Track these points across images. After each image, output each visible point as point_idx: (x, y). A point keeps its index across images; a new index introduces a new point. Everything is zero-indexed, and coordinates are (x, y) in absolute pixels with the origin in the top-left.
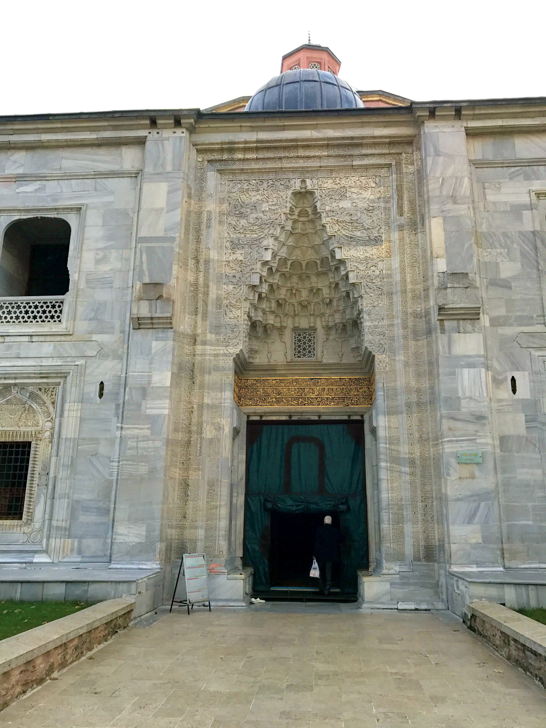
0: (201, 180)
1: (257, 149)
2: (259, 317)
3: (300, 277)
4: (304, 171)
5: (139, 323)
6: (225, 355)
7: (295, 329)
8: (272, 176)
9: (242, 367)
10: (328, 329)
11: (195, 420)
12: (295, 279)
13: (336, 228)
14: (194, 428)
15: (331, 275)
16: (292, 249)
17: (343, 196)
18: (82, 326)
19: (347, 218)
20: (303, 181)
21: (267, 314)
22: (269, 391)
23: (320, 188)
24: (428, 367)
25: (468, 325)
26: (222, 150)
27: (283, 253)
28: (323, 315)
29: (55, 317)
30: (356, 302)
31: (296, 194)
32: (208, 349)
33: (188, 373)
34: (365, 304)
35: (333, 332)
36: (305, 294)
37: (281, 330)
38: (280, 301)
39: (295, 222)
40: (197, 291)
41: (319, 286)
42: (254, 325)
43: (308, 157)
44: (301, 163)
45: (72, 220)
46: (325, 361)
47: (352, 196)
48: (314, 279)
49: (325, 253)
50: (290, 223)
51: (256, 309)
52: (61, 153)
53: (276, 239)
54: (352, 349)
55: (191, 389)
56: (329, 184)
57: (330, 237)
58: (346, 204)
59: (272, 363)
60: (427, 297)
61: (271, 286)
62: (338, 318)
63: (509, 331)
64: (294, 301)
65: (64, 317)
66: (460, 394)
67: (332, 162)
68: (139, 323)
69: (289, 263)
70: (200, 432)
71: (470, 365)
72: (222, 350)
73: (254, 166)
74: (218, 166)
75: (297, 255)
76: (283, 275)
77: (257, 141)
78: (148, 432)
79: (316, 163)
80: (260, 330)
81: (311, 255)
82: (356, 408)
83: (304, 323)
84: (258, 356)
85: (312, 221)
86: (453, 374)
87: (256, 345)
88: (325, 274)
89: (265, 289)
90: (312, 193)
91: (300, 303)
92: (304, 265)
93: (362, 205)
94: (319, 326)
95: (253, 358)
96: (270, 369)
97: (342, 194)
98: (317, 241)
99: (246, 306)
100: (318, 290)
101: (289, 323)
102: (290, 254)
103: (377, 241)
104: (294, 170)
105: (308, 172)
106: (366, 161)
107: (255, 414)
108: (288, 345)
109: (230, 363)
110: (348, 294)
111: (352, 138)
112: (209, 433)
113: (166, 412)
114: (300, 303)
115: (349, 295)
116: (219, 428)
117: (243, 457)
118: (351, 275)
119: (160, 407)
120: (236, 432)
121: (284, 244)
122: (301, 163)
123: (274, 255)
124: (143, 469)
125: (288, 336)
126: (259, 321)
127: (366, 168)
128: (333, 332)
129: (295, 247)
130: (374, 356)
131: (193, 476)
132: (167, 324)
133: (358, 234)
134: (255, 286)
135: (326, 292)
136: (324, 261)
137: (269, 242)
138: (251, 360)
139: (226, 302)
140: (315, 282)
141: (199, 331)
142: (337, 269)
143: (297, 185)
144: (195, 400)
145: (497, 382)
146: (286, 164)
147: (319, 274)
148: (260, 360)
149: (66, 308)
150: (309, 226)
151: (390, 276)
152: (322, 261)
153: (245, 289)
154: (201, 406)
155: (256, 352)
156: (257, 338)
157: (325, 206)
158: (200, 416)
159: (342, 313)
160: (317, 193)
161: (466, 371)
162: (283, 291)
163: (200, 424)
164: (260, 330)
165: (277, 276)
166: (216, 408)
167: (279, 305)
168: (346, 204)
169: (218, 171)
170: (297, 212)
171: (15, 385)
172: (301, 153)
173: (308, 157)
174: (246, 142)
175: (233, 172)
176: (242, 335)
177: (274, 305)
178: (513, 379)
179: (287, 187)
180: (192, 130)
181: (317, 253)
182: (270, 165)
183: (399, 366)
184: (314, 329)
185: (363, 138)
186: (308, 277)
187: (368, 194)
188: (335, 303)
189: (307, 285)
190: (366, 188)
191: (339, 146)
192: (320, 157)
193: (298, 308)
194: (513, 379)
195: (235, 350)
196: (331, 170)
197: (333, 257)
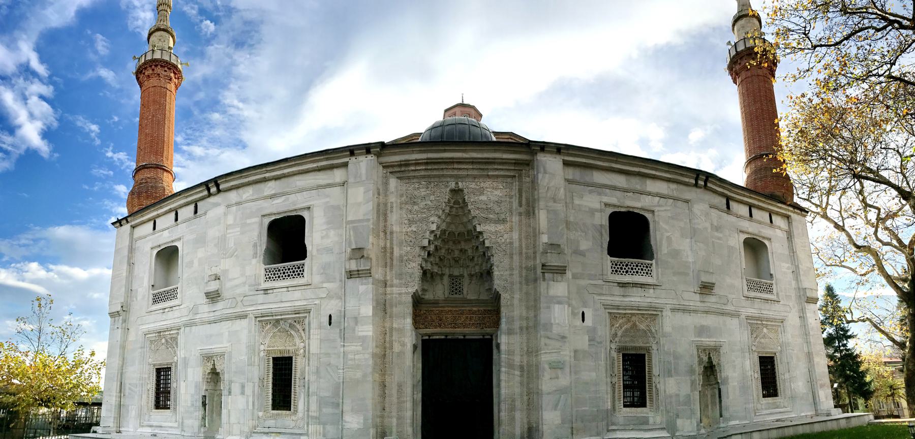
2: (429, 267)
3: (454, 242)
4: (457, 177)
5: (351, 275)
8: (437, 179)
9: (417, 301)
10: (471, 276)
11: (387, 339)
12: (451, 243)
13: (477, 212)
14: (388, 345)
15: (473, 241)
16: (449, 224)
17: (482, 193)
18: (316, 279)
19: (484, 207)
20: (457, 183)
22: (434, 317)
23: (467, 187)
24: (534, 304)
25: (559, 277)
27: (444, 226)
29: (300, 274)
30: (489, 259)
31: (452, 191)
32: (395, 290)
33: (383, 307)
34: (495, 260)
35: (474, 278)
36: (457, 253)
37: (442, 275)
39: (451, 207)
41: (466, 248)
42: (425, 272)
43: (460, 169)
44: (456, 172)
46: (468, 298)
47: (488, 195)
48: (463, 243)
49: (470, 227)
50: (448, 208)
51: (426, 261)
53: (439, 217)
55: (384, 318)
56: (473, 186)
57: (474, 217)
58: (483, 198)
60: (535, 258)
61: (436, 246)
62: (477, 269)
63: (583, 282)
65: (305, 274)
66: (552, 321)
67: (475, 173)
68: (351, 275)
70: (391, 348)
71: (559, 303)
72: (404, 290)
75: (453, 228)
76: (443, 240)
77: (427, 159)
78: (360, 348)
79: (465, 173)
80: (429, 275)
81: (461, 229)
82: (489, 330)
83: (456, 272)
85: (462, 208)
86: (549, 307)
88: (470, 240)
89: (432, 248)
90: (462, 190)
91: (454, 259)
93: (493, 198)
96: (435, 303)
97: (481, 192)
98: (465, 220)
99: (419, 260)
101: (447, 271)
102: (448, 227)
103: (504, 221)
104: (451, 176)
106: (496, 173)
107: (426, 335)
108: (446, 287)
109: (410, 299)
110: (484, 253)
112: (397, 348)
113: (371, 334)
114: (454, 259)
115: (486, 255)
116: (403, 345)
117: (420, 365)
118: (486, 242)
119: (367, 330)
120: (415, 347)
122: (456, 172)
123: (438, 228)
124: (359, 375)
125: (446, 279)
127: (497, 176)
128: (474, 278)
129: (450, 223)
131: (388, 379)
132: (368, 273)
133: (491, 216)
134: (424, 247)
135: (470, 251)
136: (469, 232)
139: (405, 258)
140: (463, 245)
141: (388, 278)
142: (478, 237)
143: (452, 185)
144: (387, 325)
145: (574, 314)
146: (445, 172)
147: (466, 241)
148: (429, 296)
149: (306, 268)
150: (460, 210)
152: (468, 232)
154: (391, 329)
156: (427, 281)
157: (470, 199)
158: (391, 336)
160: (465, 191)
161: (557, 306)
162: (443, 251)
163: (391, 342)
164: (429, 275)
165: (440, 241)
166: (401, 331)
167: (441, 260)
168: (483, 198)
170: (452, 201)
172: (456, 166)
173: (460, 169)
176: (417, 279)
177: (437, 259)
179: (447, 186)
182: (435, 173)
183: (516, 302)
184: (462, 276)
185: (495, 159)
186: (459, 242)
187: (498, 193)
188: (476, 259)
190: (496, 189)
191: (479, 163)
192: (467, 169)
193: (452, 262)
194: (583, 314)
195: (412, 290)
196: (475, 177)
197: (475, 230)
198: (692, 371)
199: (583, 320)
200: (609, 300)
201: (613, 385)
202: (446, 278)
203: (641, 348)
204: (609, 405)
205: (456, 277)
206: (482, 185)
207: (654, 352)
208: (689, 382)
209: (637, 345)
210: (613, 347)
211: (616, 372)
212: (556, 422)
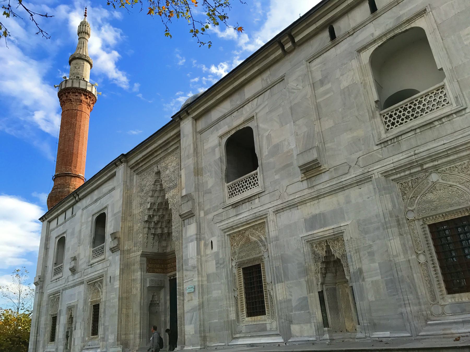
0: (131, 180)
1: (144, 159)
2: (159, 231)
6: (138, 255)
26: (136, 165)
40: (131, 229)
45: (105, 211)
52: (103, 186)
53: (152, 196)
69: (164, 203)
73: (144, 167)
74: (137, 172)
77: (142, 157)
87: (164, 244)
93: (172, 170)
105: (158, 162)
111: (165, 141)
112: (134, 291)
116: (137, 289)
121: (158, 197)
137: (149, 199)
138: (165, 251)
143: (156, 170)
146: (152, 162)
151: (179, 201)
153: (143, 223)
168: (168, 172)
169: (137, 174)
171: (96, 282)
174: (140, 159)
175: (140, 173)
178: (212, 242)
180: (127, 162)
182: (148, 164)
185: (168, 139)
192: (159, 154)
196: (164, 157)
198: (306, 271)
199: (212, 248)
200: (224, 224)
201: (236, 299)
203: (254, 259)
204: (233, 316)
206: (167, 162)
207: (266, 260)
208: (304, 283)
209: (251, 257)
210: (234, 265)
211: (238, 286)
212: (191, 333)
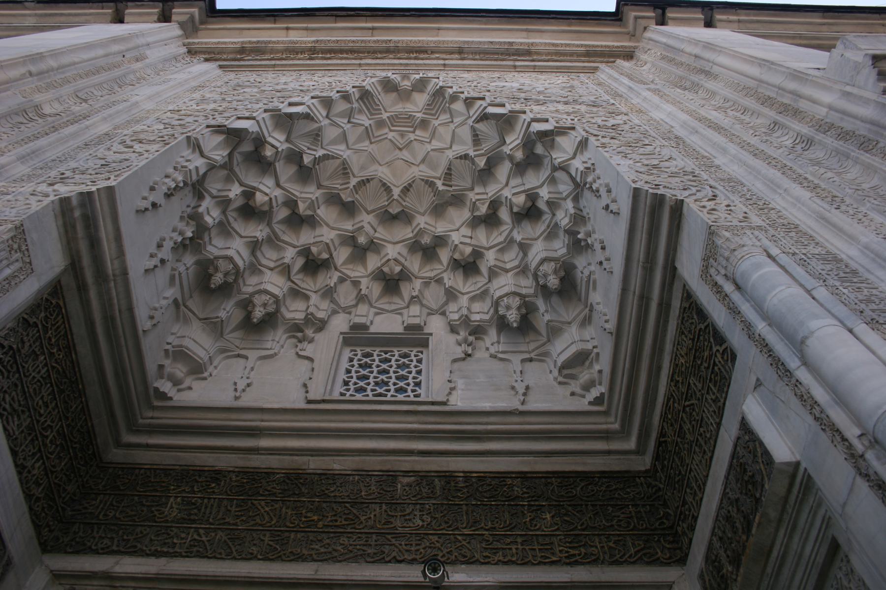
7: (357, 337)
12: (366, 219)
21: (261, 272)
28: (451, 295)
38: (314, 250)
46: (458, 402)
54: (563, 367)
59: (247, 401)
64: (356, 272)
83: (387, 324)
84: (196, 385)
87: (198, 341)
92: (396, 192)
94: (436, 326)
95: (176, 382)
100: (441, 241)
125: (325, 345)
126: (230, 259)
130: (678, 208)
138: (166, 387)
155: (197, 369)
159: (517, 274)
181: (433, 167)
189: (406, 233)
202: (325, 345)
205: (387, 341)
